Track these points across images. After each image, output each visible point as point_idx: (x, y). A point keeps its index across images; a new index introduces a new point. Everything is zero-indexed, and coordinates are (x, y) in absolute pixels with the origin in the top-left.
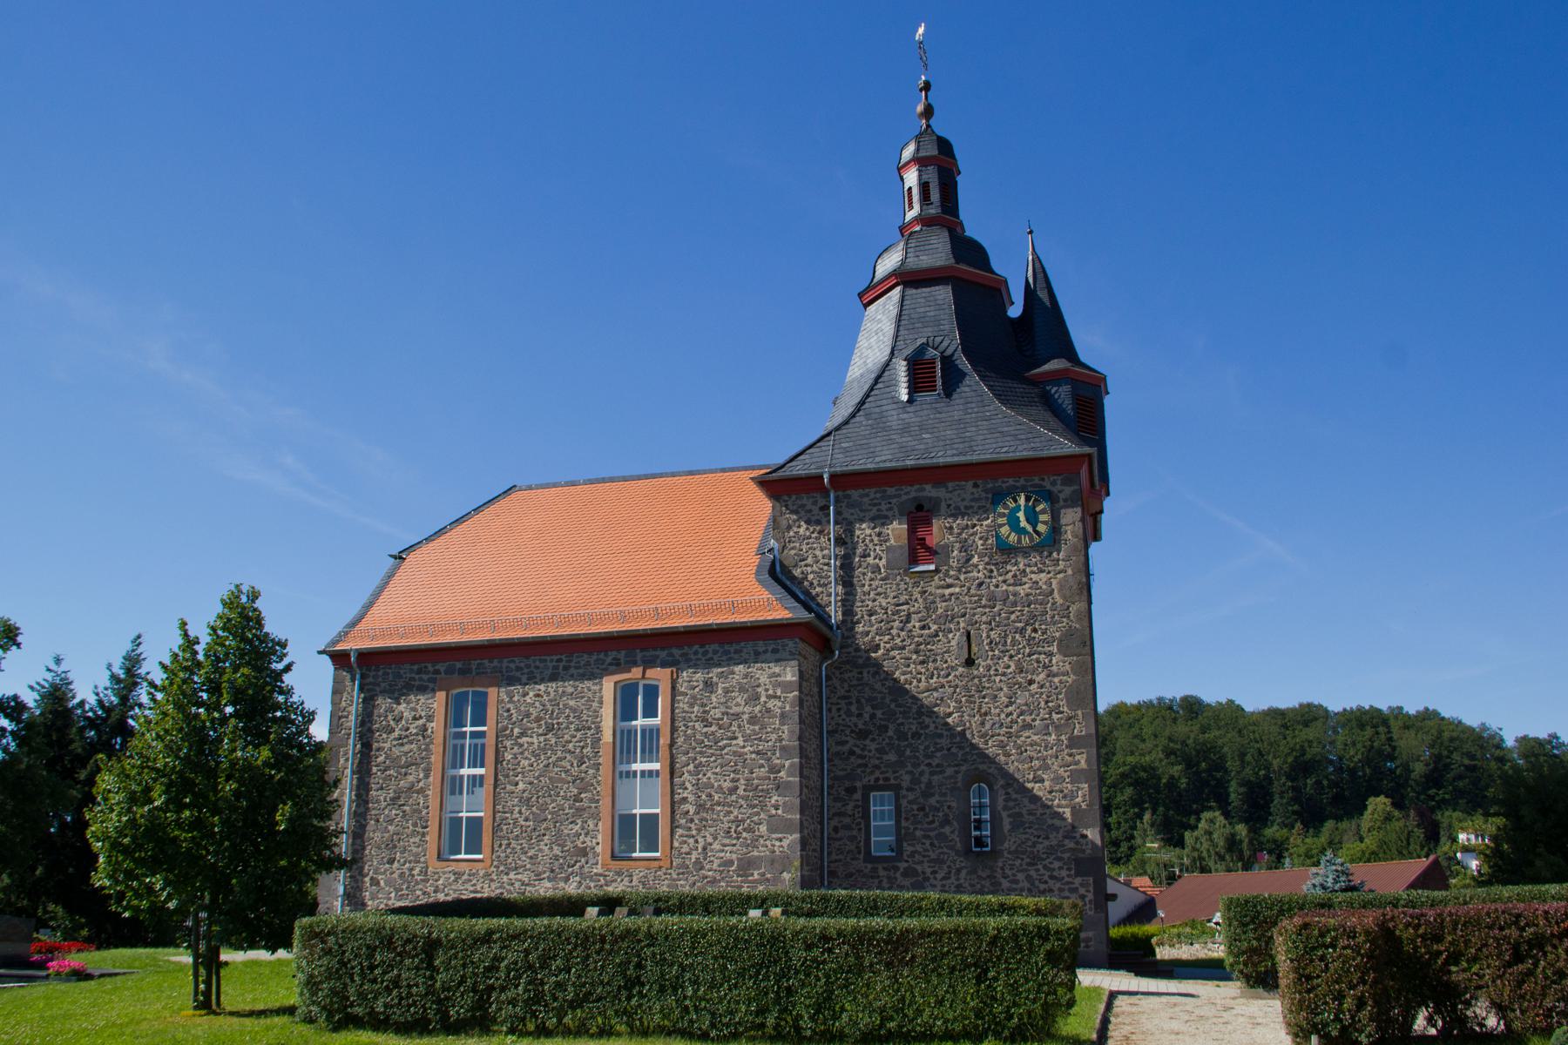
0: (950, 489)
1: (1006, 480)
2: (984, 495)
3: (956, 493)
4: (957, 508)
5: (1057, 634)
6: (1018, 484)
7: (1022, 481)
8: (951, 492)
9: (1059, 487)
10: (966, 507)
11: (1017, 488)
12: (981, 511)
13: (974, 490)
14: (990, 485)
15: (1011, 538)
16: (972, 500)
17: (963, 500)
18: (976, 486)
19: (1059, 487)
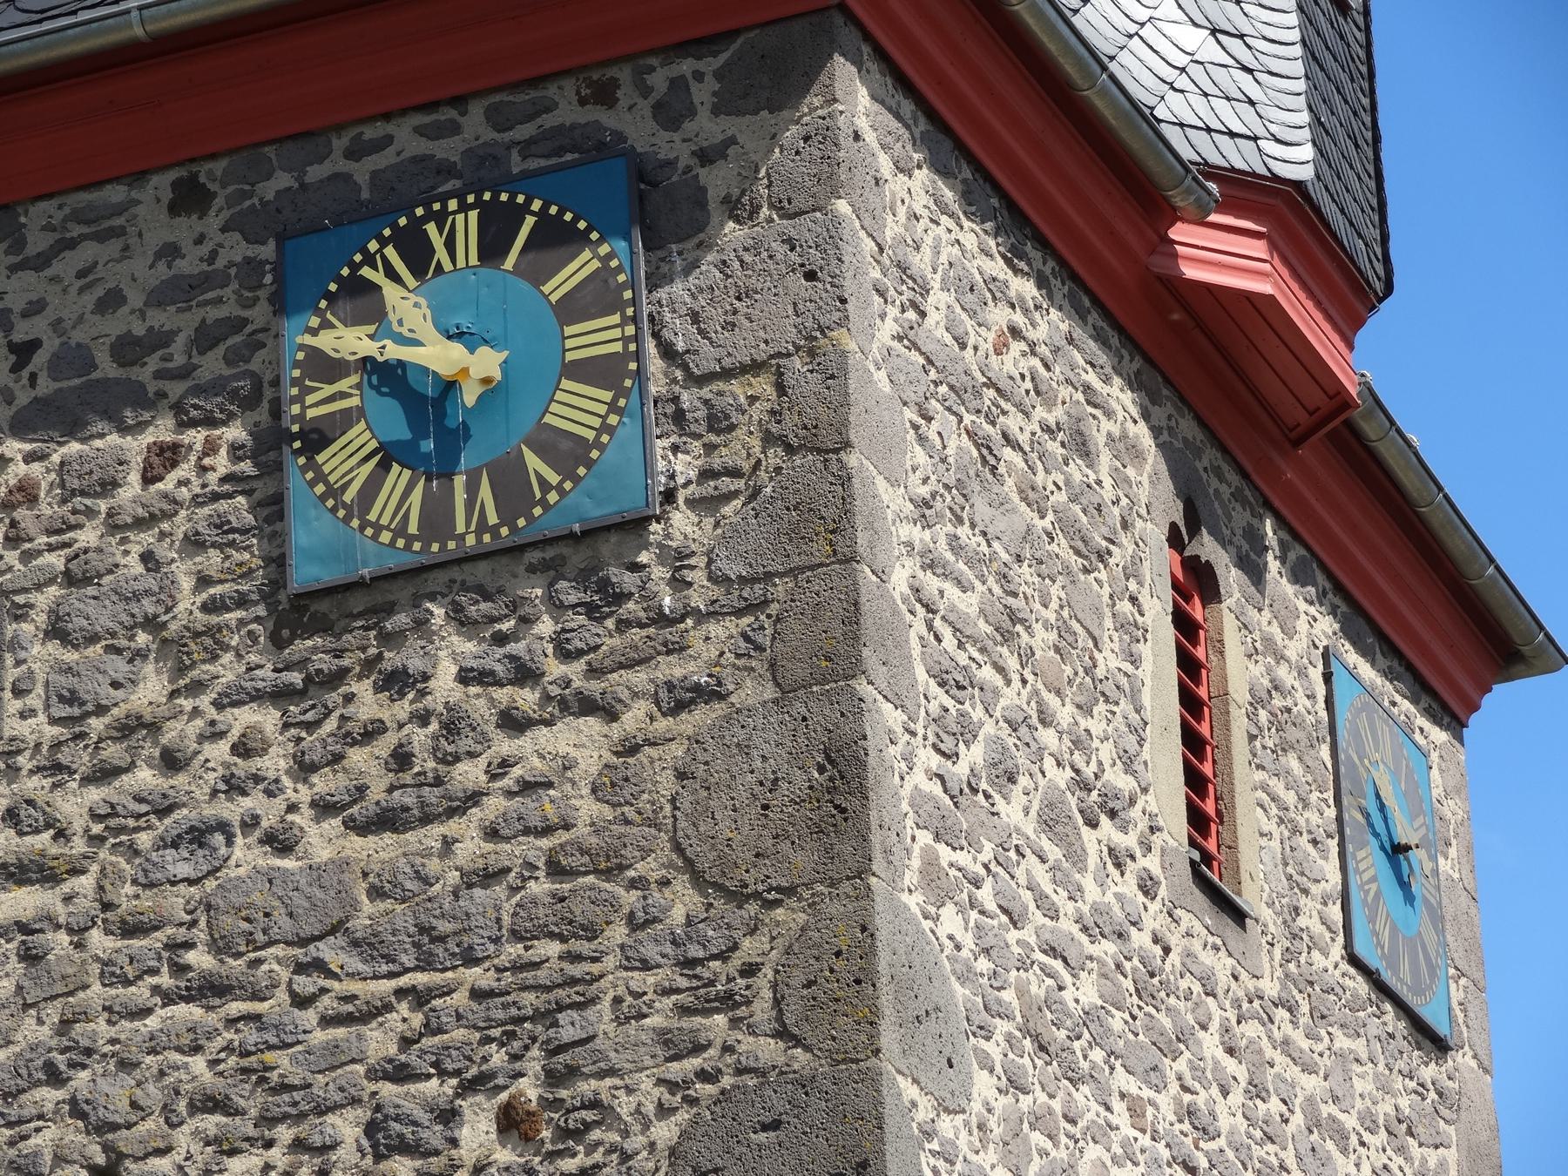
0: (37, 242)
1: (370, 132)
2: (236, 249)
3: (66, 266)
4: (75, 360)
5: (665, 1132)
6: (448, 149)
7: (475, 124)
8: (41, 262)
9: (707, 127)
10: (128, 350)
11: (446, 170)
12: (212, 365)
13: (183, 229)
14: (283, 180)
15: (383, 508)
16: (159, 298)
17: (112, 301)
18: (190, 198)
19: (707, 127)
